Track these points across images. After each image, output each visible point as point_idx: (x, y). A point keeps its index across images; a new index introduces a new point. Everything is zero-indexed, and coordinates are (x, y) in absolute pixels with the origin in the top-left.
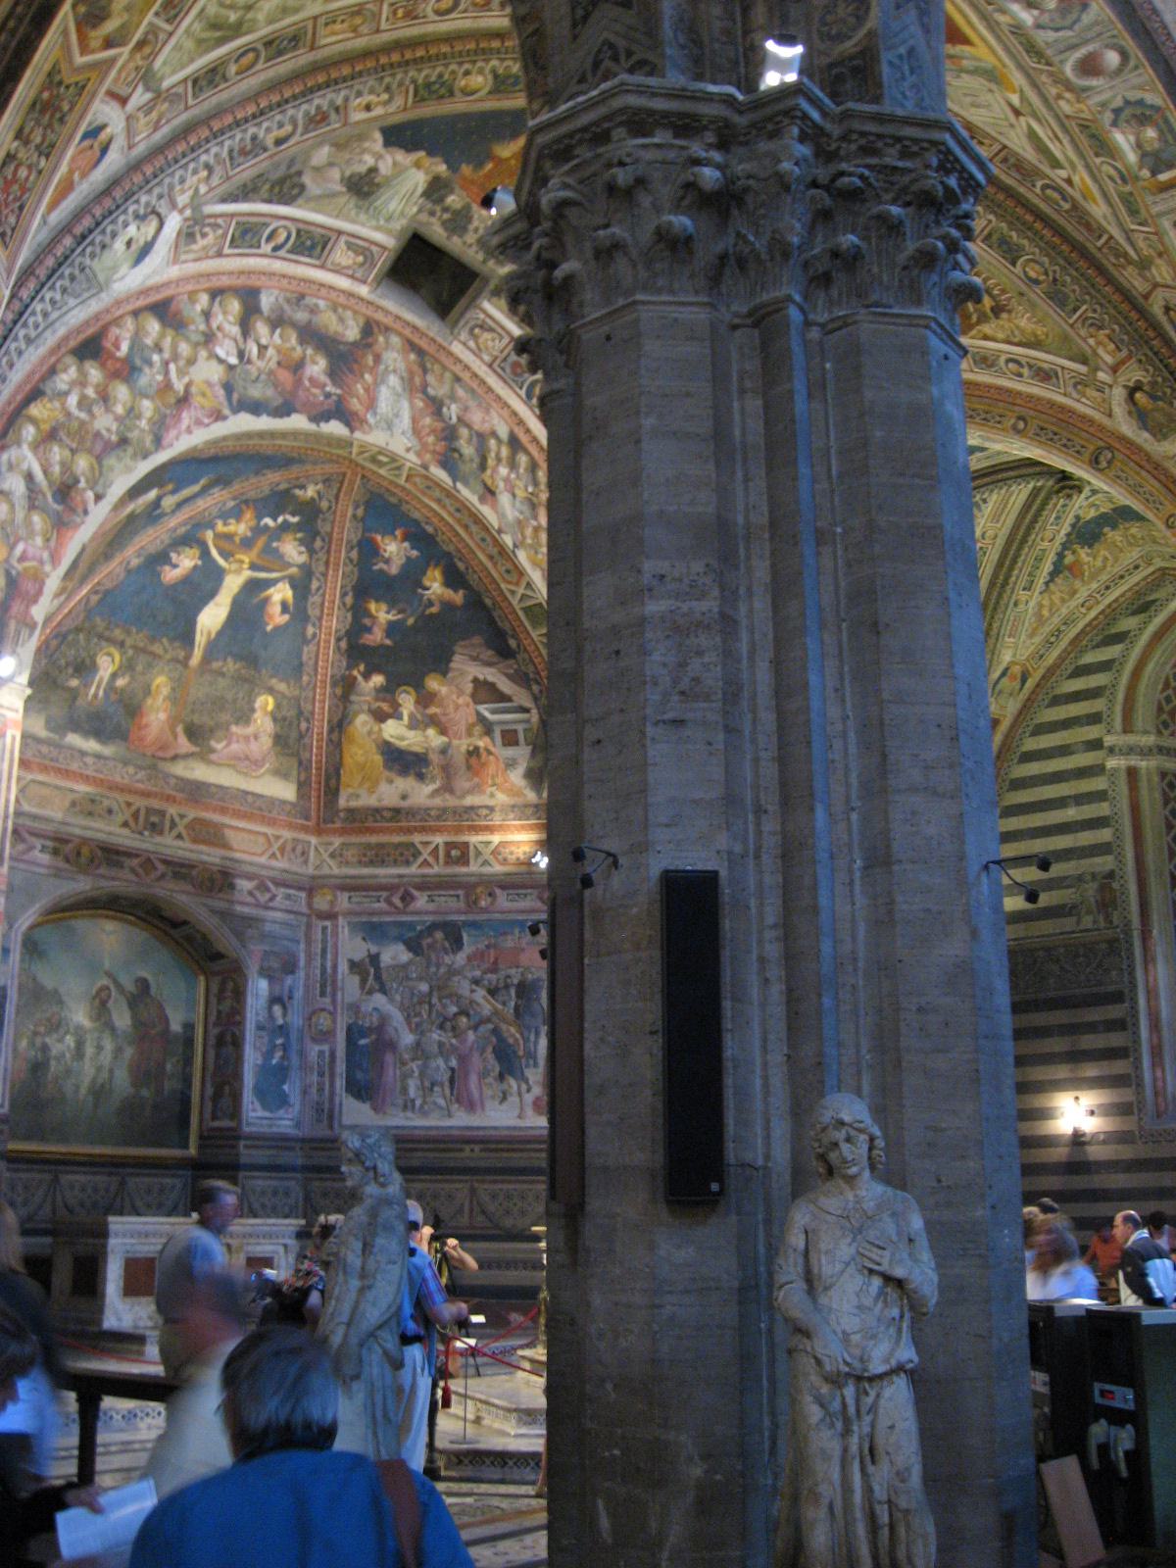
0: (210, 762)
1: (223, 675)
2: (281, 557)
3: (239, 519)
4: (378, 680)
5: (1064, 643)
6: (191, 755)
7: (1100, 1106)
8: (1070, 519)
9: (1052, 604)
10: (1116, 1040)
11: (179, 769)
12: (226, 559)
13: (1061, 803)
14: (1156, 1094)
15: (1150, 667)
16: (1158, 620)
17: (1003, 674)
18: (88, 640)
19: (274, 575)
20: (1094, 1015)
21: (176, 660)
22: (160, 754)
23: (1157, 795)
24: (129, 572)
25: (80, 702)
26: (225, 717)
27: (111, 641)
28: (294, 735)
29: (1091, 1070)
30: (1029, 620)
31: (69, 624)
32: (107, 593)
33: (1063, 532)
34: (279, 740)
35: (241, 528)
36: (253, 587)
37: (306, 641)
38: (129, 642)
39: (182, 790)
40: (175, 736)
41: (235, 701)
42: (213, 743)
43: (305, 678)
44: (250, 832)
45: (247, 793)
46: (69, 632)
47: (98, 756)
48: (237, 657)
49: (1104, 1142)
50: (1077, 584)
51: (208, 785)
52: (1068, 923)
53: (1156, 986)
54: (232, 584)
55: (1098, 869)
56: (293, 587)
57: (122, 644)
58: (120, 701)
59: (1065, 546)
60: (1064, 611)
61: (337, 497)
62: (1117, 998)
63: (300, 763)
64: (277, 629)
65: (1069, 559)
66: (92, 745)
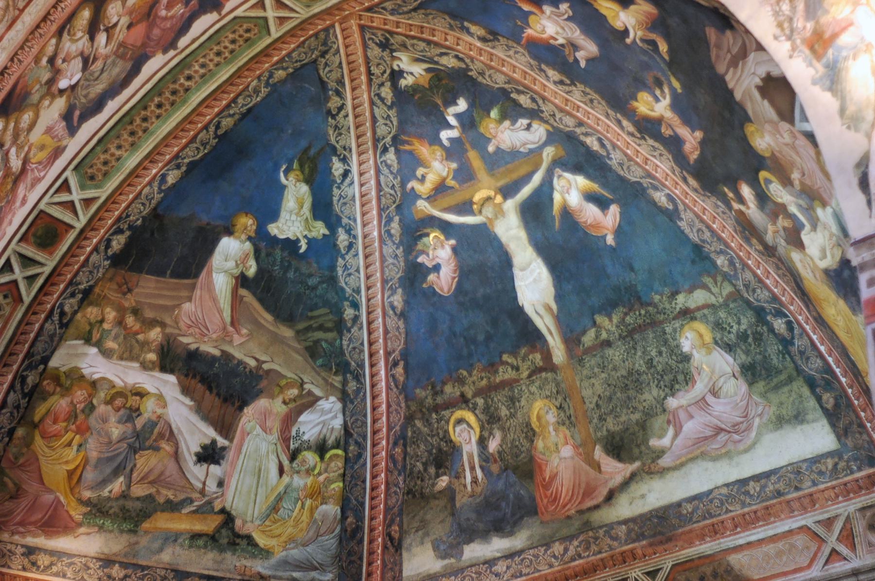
0: (663, 472)
1: (608, 344)
2: (514, 154)
3: (419, 162)
4: (746, 191)
6: (633, 477)
11: (625, 508)
12: (471, 213)
18: (427, 422)
19: (537, 179)
21: (536, 371)
22: (589, 503)
24: (402, 315)
25: (461, 500)
26: (650, 395)
27: (451, 405)
28: (773, 349)
31: (398, 419)
32: (405, 355)
34: (751, 372)
35: (437, 168)
36: (535, 212)
37: (672, 215)
38: (469, 392)
39: (640, 536)
40: (597, 467)
41: (650, 363)
42: (654, 442)
43: (720, 261)
44: (774, 539)
45: (744, 482)
46: (404, 428)
47: (510, 555)
48: (607, 308)
51: (679, 504)
54: (510, 230)
56: (577, 169)
57: (464, 401)
58: (506, 469)
61: (437, 44)
63: (811, 384)
64: (619, 232)
66: (498, 545)
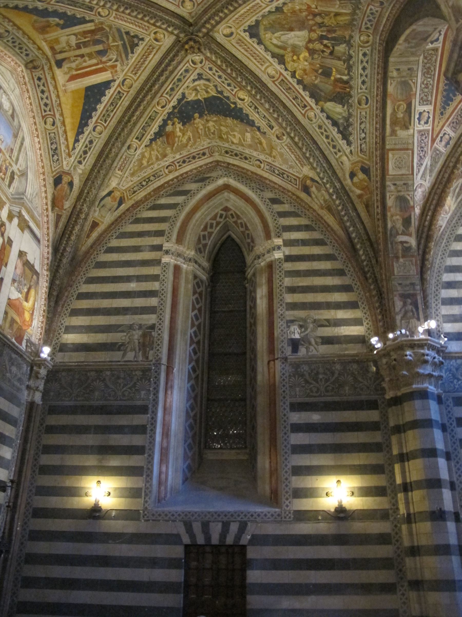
5: (150, 189)
7: (116, 489)
8: (178, 96)
9: (150, 158)
10: (137, 440)
13: (128, 279)
14: (160, 483)
15: (198, 215)
16: (210, 188)
17: (109, 194)
20: (123, 420)
23: (190, 286)
29: (115, 461)
30: (133, 165)
33: (172, 104)
49: (115, 518)
50: (168, 150)
52: (117, 356)
53: (171, 406)
55: (143, 323)
59: (170, 116)
60: (156, 167)
62: (143, 410)
65: (169, 128)
